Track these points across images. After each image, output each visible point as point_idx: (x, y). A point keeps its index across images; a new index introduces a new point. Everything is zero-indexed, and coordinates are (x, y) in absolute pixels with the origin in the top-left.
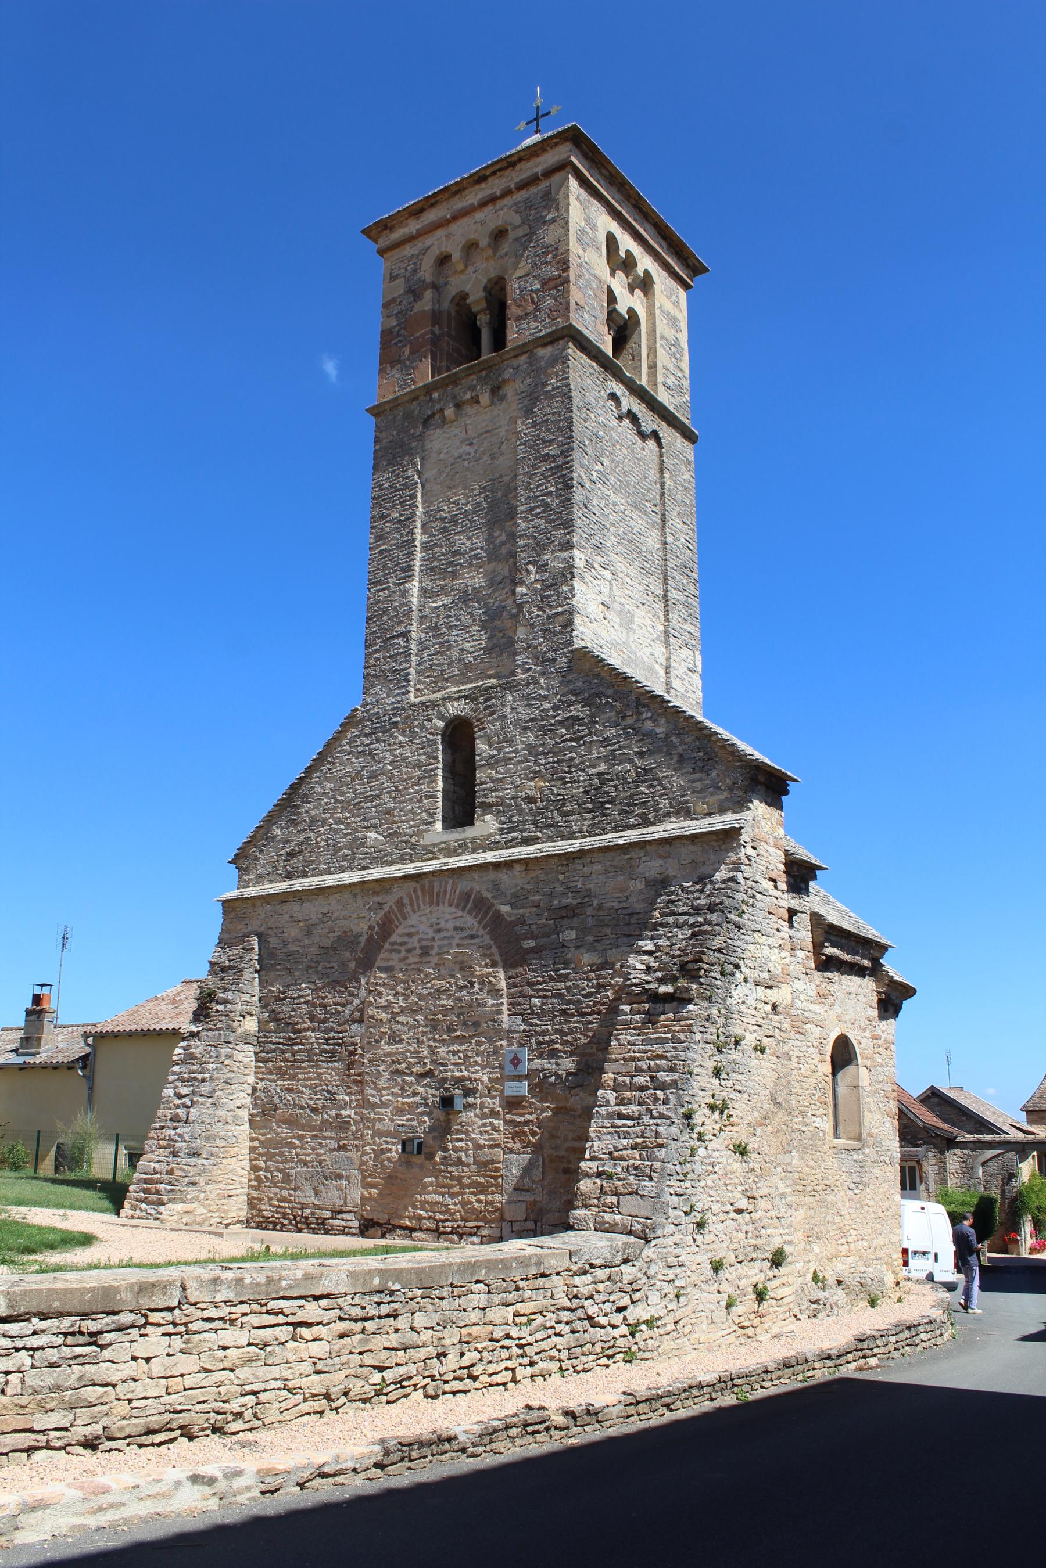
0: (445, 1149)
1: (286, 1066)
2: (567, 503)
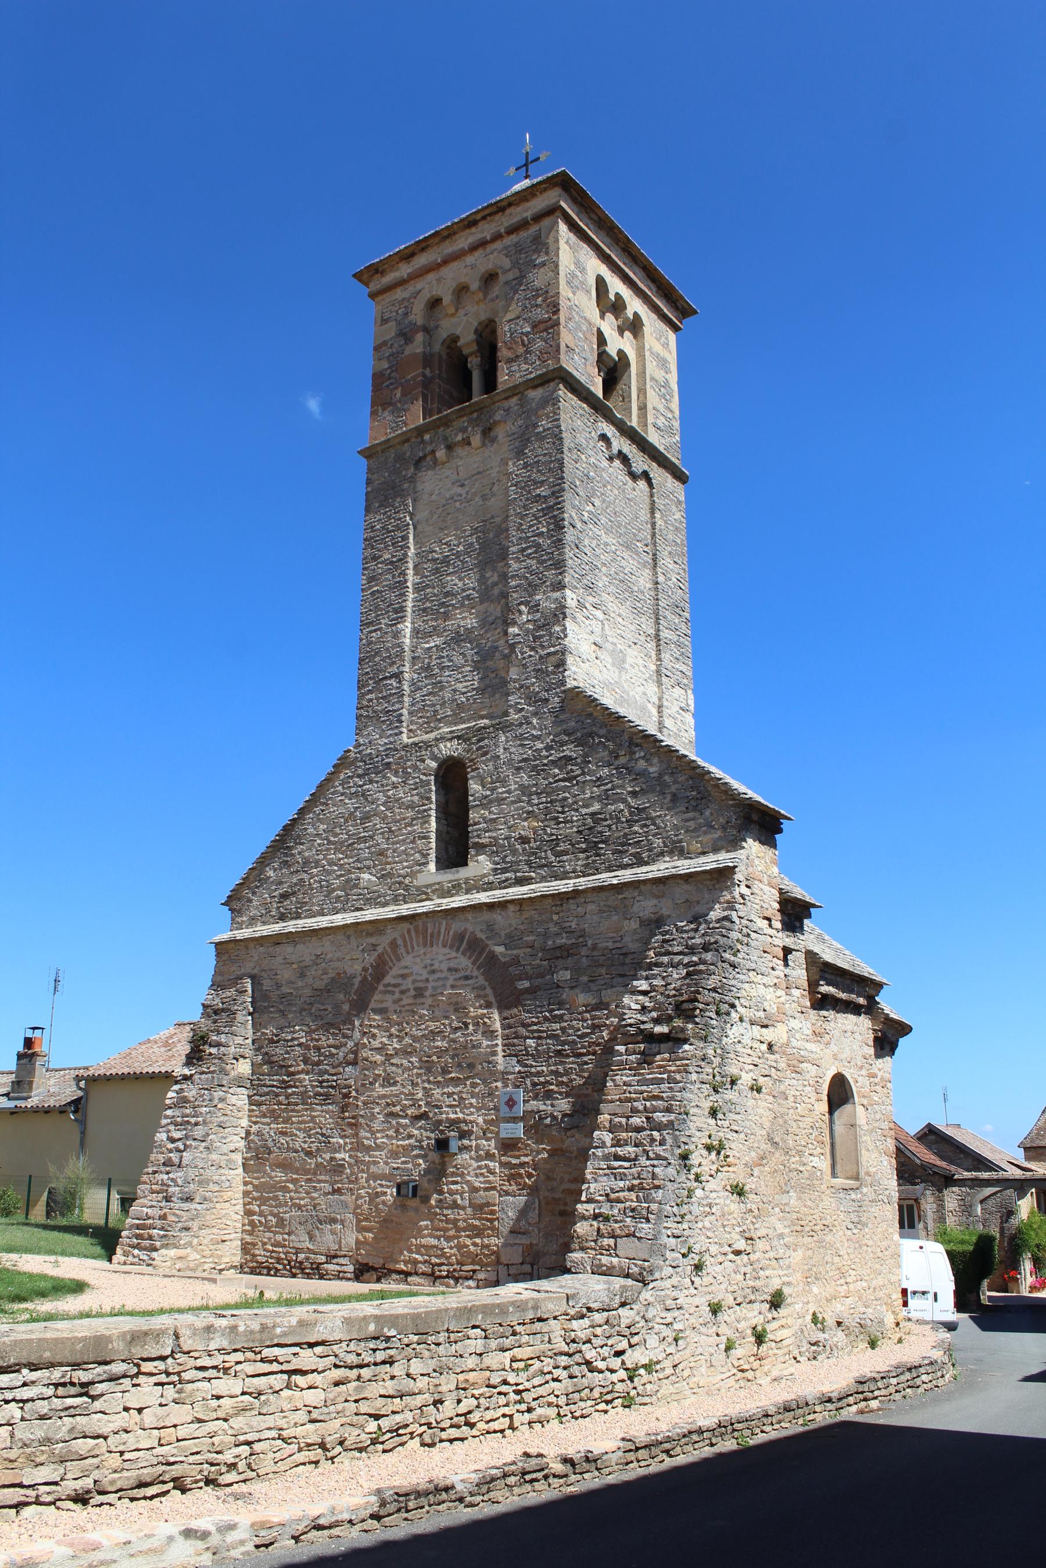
0: (441, 1192)
1: (280, 1109)
2: (559, 543)
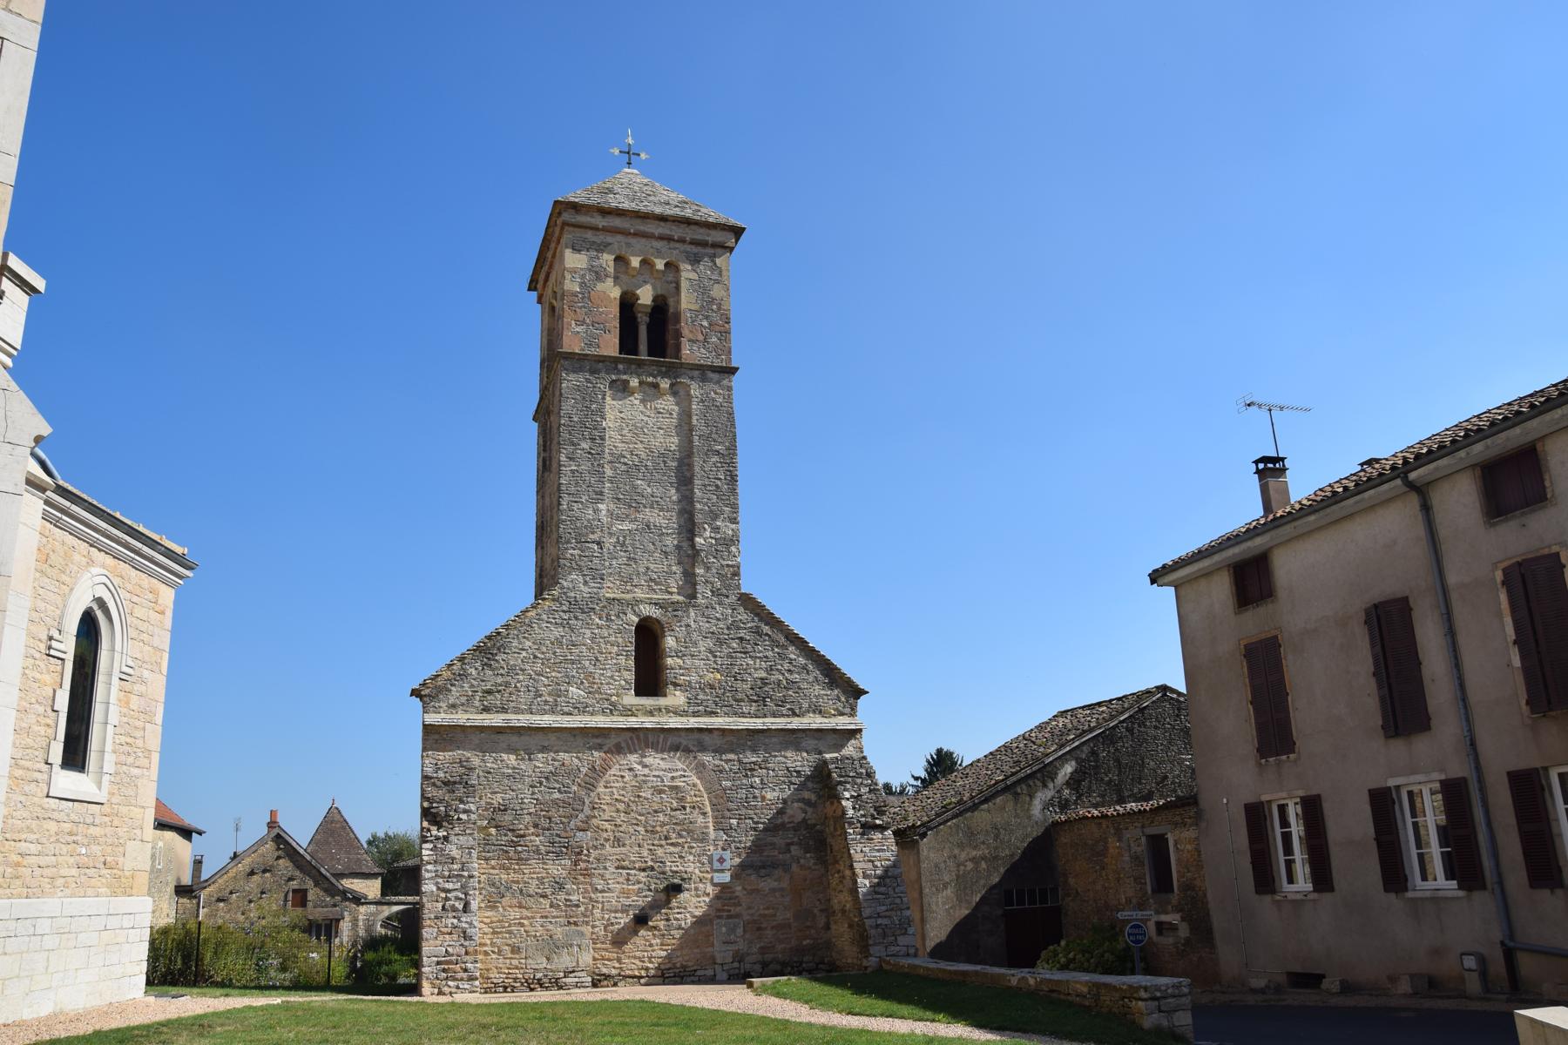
1: (511, 864)
2: (733, 491)
